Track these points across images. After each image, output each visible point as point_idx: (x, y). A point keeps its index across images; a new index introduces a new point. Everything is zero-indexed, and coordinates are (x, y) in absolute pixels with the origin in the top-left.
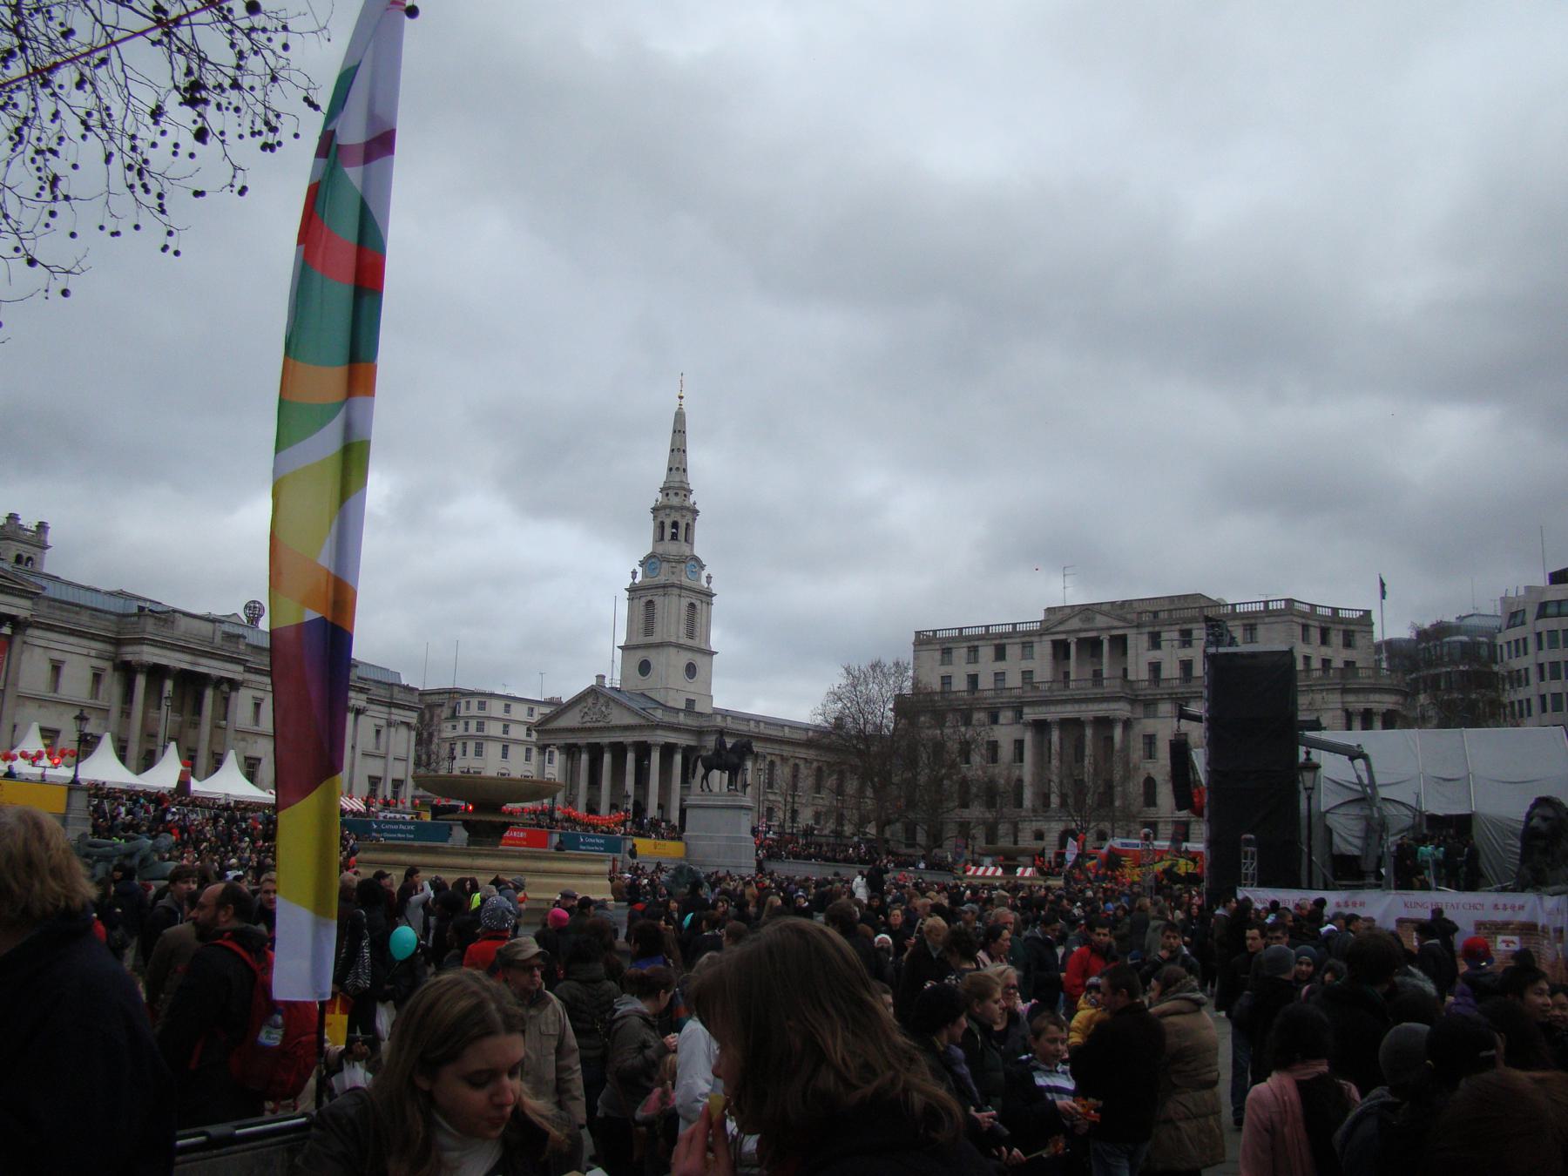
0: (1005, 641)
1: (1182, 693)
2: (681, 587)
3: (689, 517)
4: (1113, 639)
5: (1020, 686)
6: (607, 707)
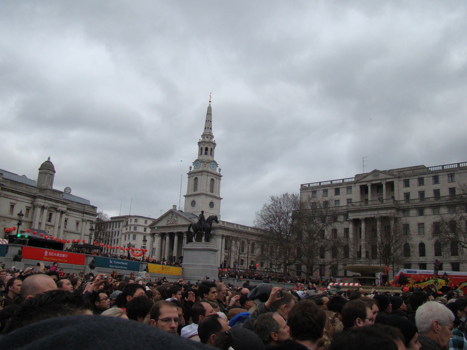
0: (339, 187)
1: (421, 205)
2: (208, 172)
3: (212, 146)
4: (387, 184)
5: (346, 205)
6: (176, 218)
